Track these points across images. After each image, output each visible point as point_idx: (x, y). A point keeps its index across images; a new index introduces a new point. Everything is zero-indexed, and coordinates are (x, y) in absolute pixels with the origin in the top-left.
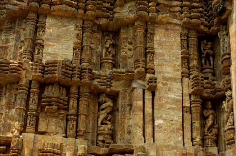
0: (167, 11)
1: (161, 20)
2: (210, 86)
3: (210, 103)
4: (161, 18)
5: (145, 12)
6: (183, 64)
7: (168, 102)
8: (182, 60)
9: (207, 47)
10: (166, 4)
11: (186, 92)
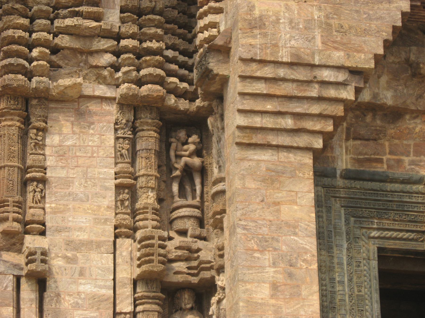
0: (82, 64)
1: (62, 93)
2: (185, 253)
3: (189, 296)
4: (63, 88)
5: (20, 76)
6: (119, 204)
7: (77, 303)
8: (117, 194)
9: (186, 151)
10: (76, 49)
11: (125, 276)
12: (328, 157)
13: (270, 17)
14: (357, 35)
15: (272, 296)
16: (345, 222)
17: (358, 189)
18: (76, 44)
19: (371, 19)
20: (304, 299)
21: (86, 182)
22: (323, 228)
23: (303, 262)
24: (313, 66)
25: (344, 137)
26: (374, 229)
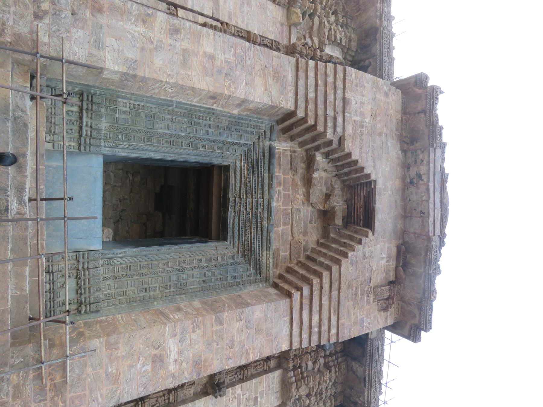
13: (365, 91)
14: (360, 143)
15: (205, 53)
17: (264, 155)
18: (315, 28)
20: (203, 77)
21: (250, 15)
23: (229, 84)
24: (344, 112)
26: (241, 164)
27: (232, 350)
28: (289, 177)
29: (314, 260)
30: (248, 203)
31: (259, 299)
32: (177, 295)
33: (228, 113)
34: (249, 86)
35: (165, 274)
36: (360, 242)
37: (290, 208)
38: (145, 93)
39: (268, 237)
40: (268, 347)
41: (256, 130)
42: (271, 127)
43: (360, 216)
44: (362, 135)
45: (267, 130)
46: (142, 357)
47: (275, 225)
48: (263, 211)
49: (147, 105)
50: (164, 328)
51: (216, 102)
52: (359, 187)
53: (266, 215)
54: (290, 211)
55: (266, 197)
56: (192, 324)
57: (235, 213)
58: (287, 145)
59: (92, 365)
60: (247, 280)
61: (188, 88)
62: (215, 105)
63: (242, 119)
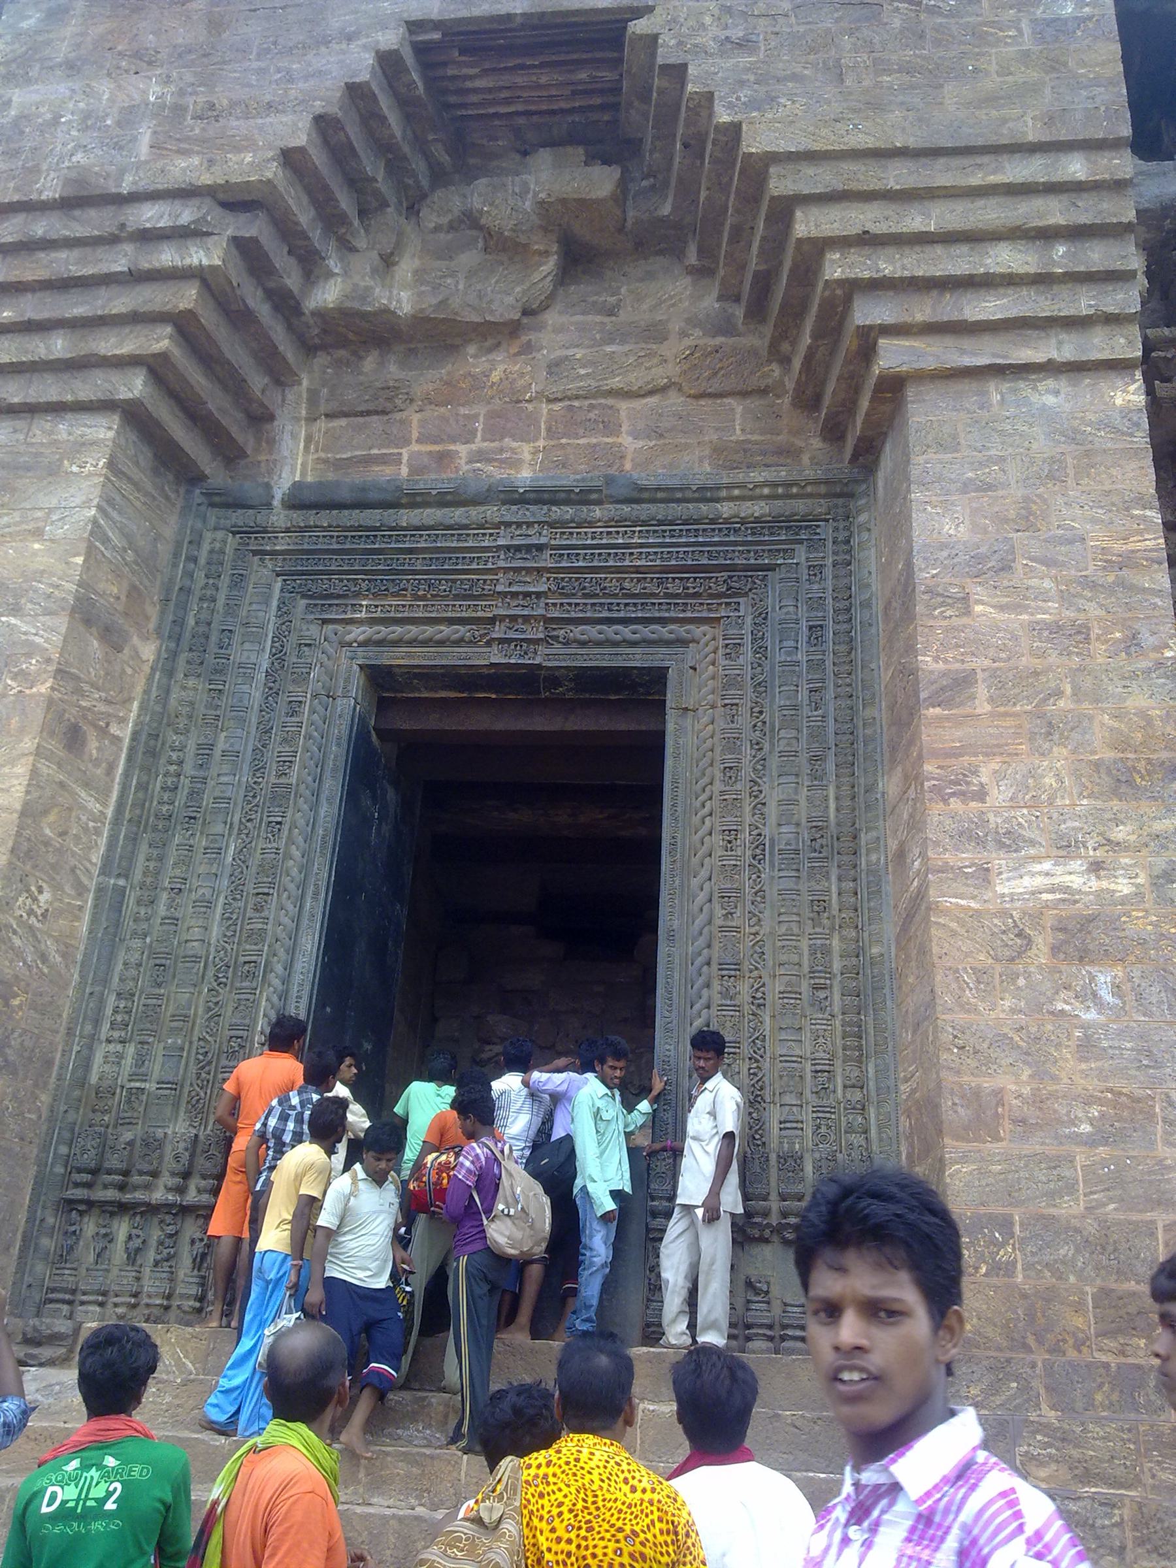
12: (259, 462)
16: (279, 608)
17: (324, 529)
19: (291, 80)
22: (209, 624)
25: (304, 412)
27: (1096, 631)
28: (416, 418)
29: (764, 283)
30: (514, 589)
31: (900, 525)
32: (855, 866)
33: (150, 678)
34: (23, 601)
35: (767, 913)
36: (679, 72)
37: (545, 408)
38: (66, 986)
39: (660, 495)
40: (1114, 471)
41: (228, 565)
42: (212, 505)
43: (580, 82)
44: (212, 106)
45: (228, 523)
46: (1051, 1001)
47: (612, 471)
48: (552, 525)
49: (116, 979)
50: (946, 912)
51: (96, 726)
52: (453, 99)
53: (568, 512)
54: (557, 407)
55: (492, 512)
56: (945, 801)
57: (556, 638)
58: (287, 437)
59: (1051, 1195)
60: (835, 577)
61: (27, 832)
62: (114, 729)
63: (179, 623)
